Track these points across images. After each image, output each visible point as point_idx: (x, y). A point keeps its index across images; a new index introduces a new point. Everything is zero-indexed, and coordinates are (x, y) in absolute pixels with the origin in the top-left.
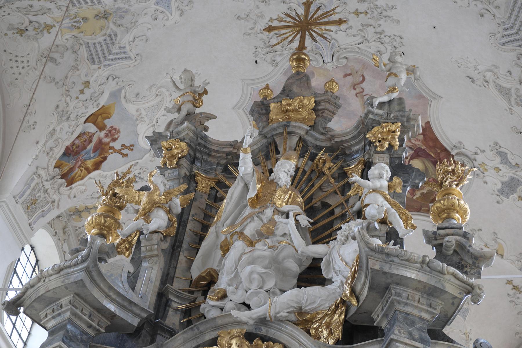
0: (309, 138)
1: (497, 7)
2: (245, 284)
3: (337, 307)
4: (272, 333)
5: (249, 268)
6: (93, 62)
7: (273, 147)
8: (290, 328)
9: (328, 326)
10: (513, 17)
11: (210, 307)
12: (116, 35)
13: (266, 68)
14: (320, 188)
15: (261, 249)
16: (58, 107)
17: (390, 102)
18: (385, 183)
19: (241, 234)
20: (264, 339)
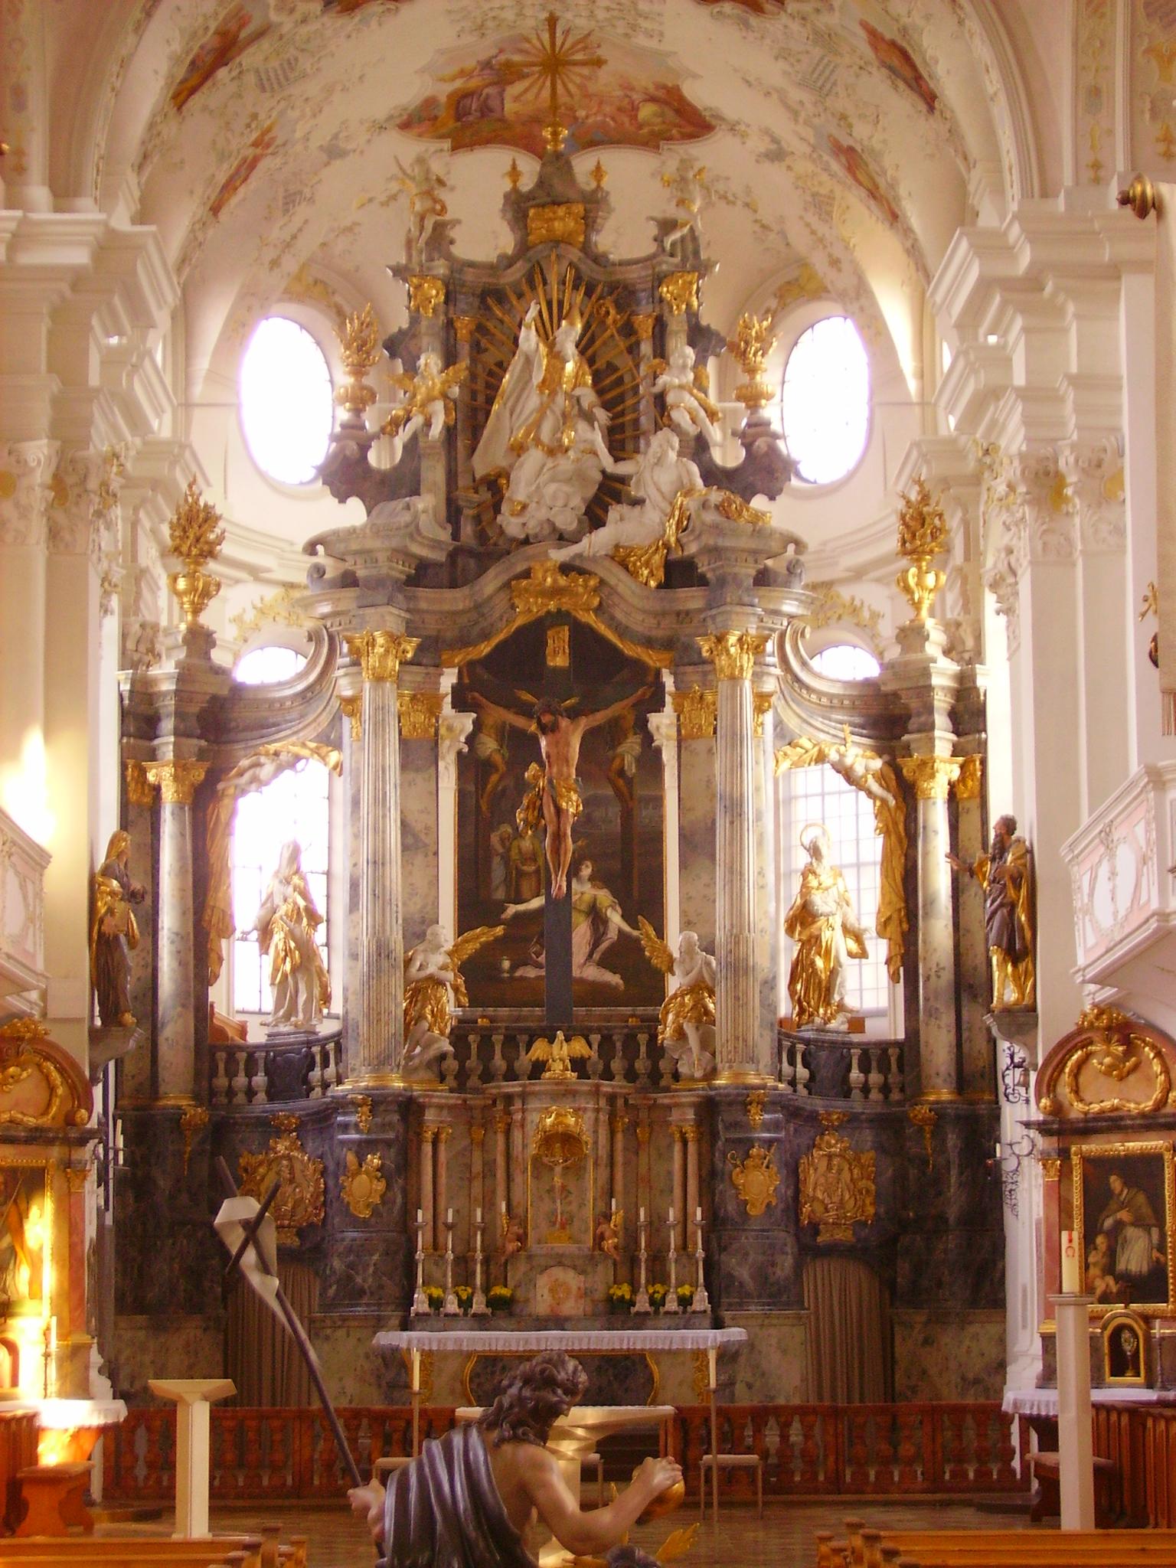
0: (583, 267)
1: (799, 61)
2: (548, 500)
3: (657, 549)
4: (587, 566)
5: (553, 487)
6: (263, 90)
7: (538, 270)
8: (607, 563)
9: (647, 564)
10: (817, 73)
11: (511, 524)
12: (296, 59)
13: (469, 39)
14: (604, 343)
15: (565, 464)
16: (214, 142)
17: (683, 239)
18: (691, 376)
19: (538, 441)
20: (582, 572)
